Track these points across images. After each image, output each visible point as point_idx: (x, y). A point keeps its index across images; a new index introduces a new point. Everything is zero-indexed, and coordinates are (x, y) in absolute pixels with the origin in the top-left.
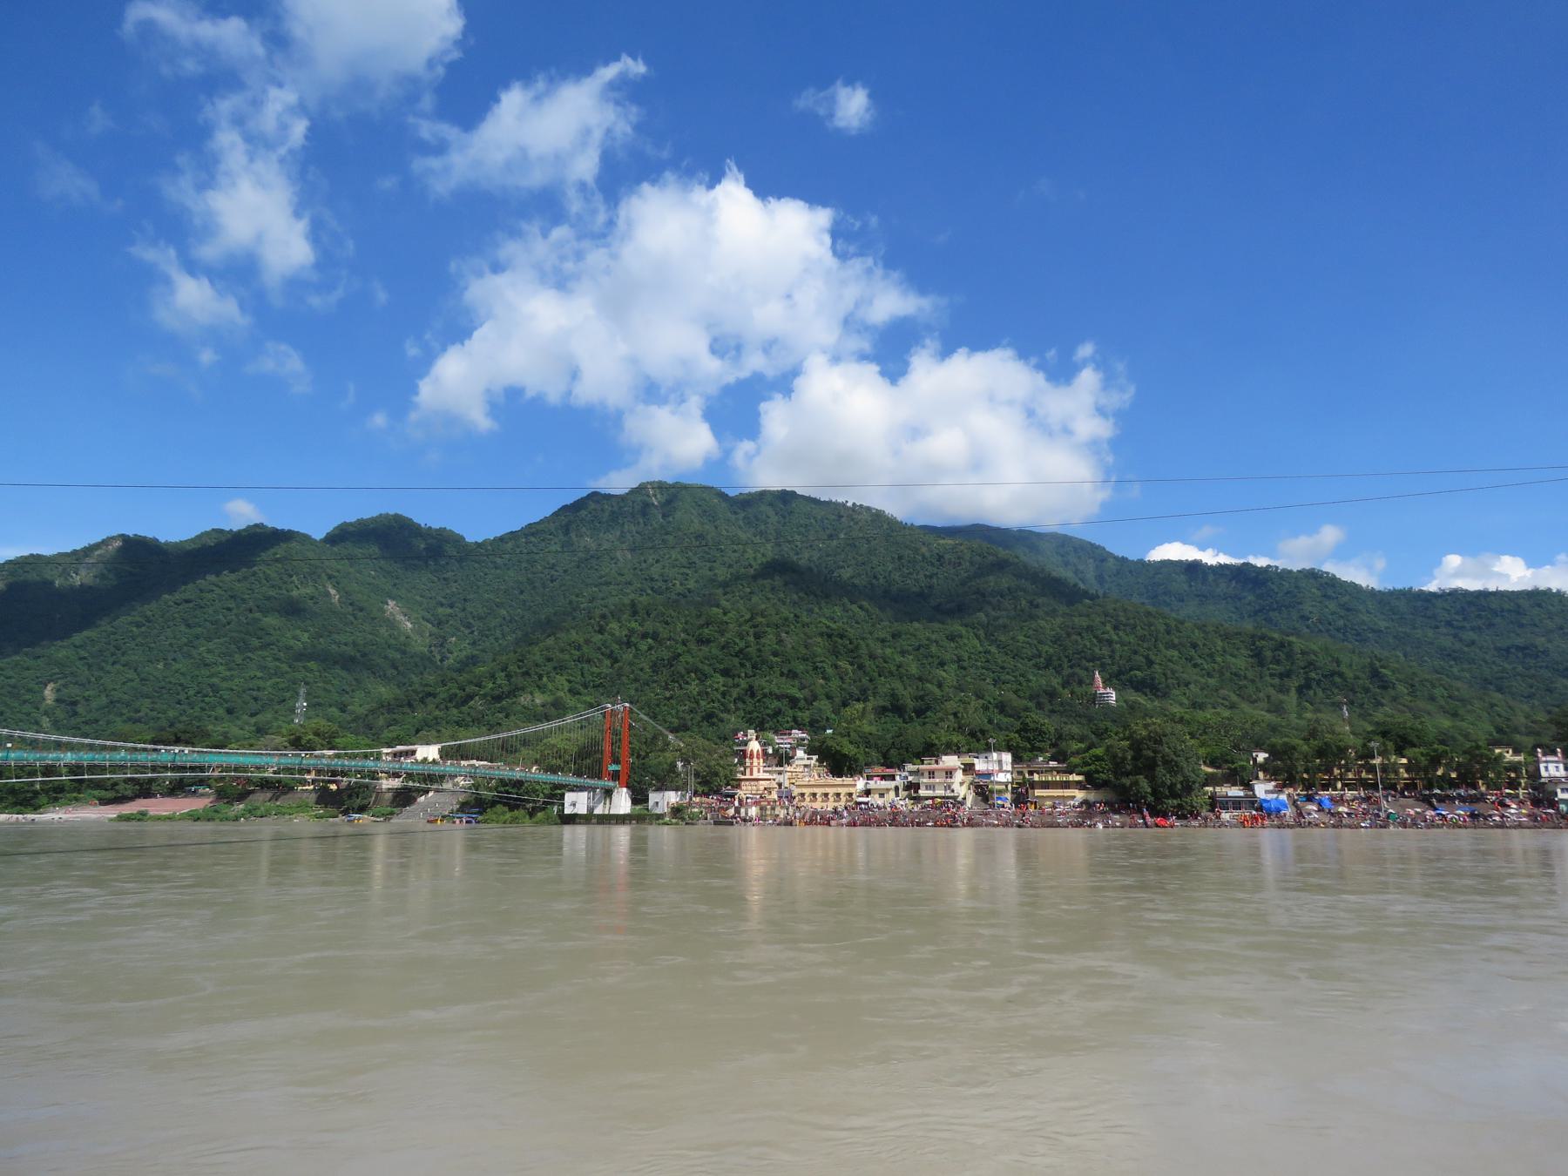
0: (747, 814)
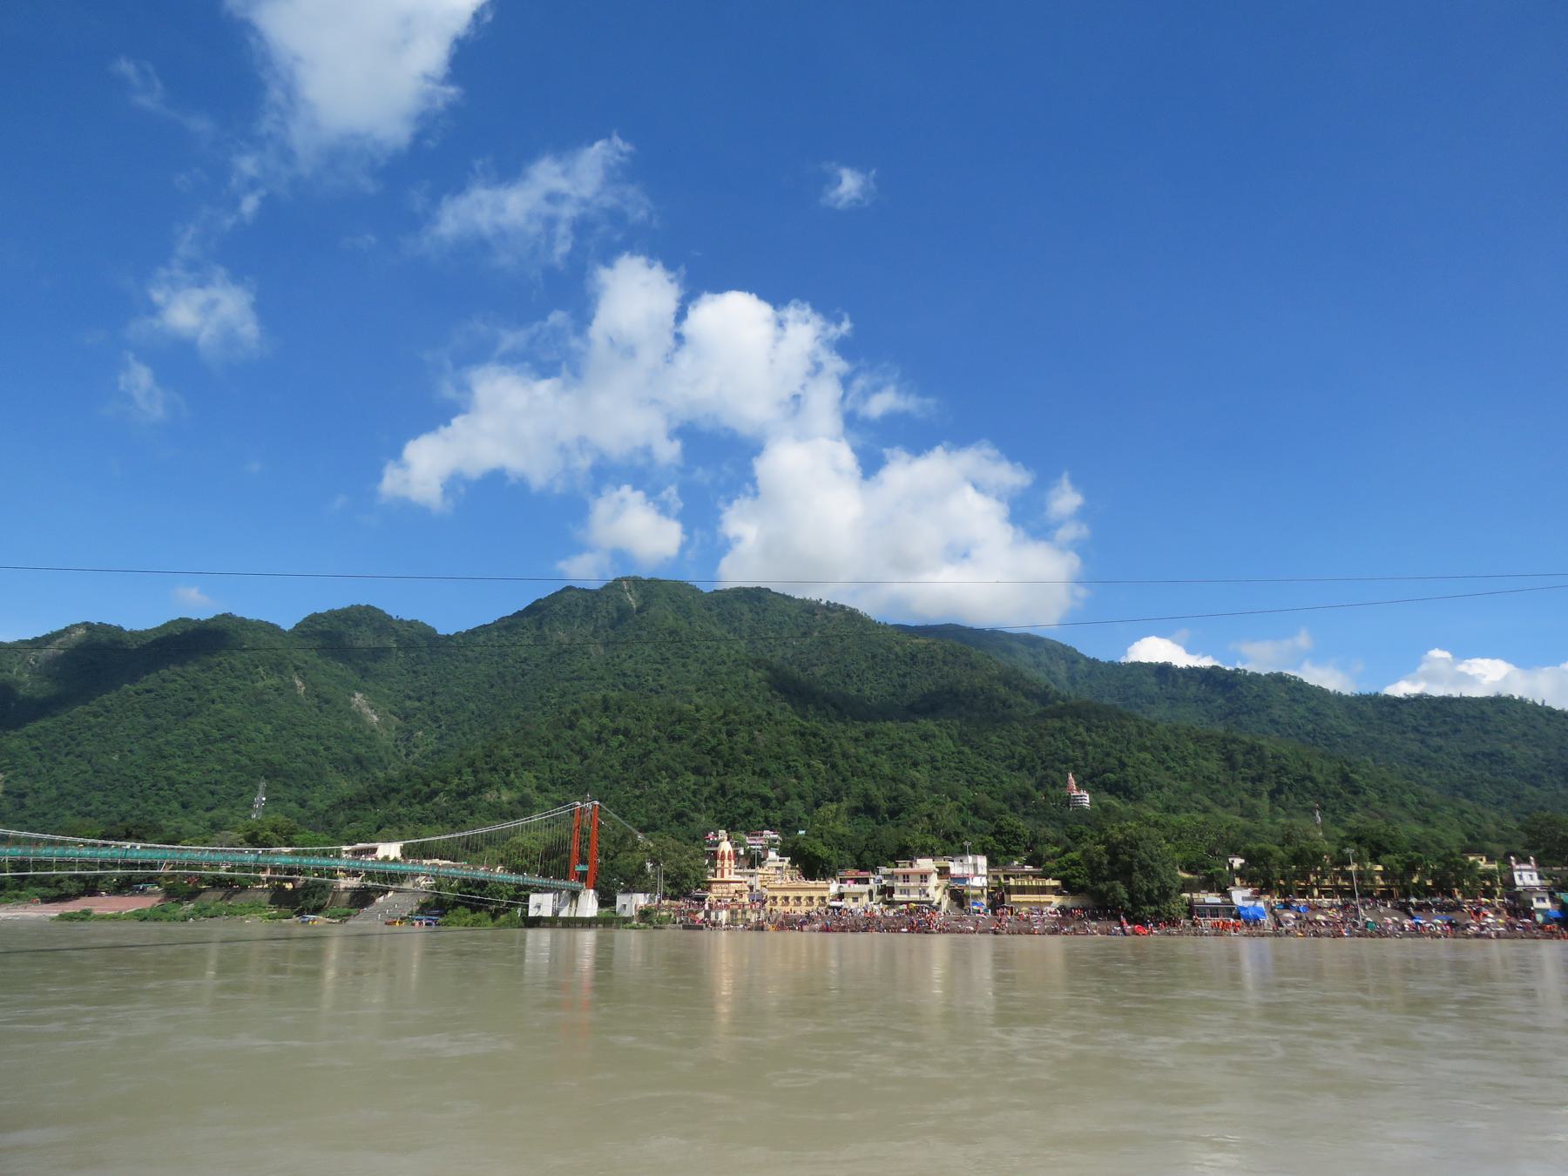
0: (717, 918)
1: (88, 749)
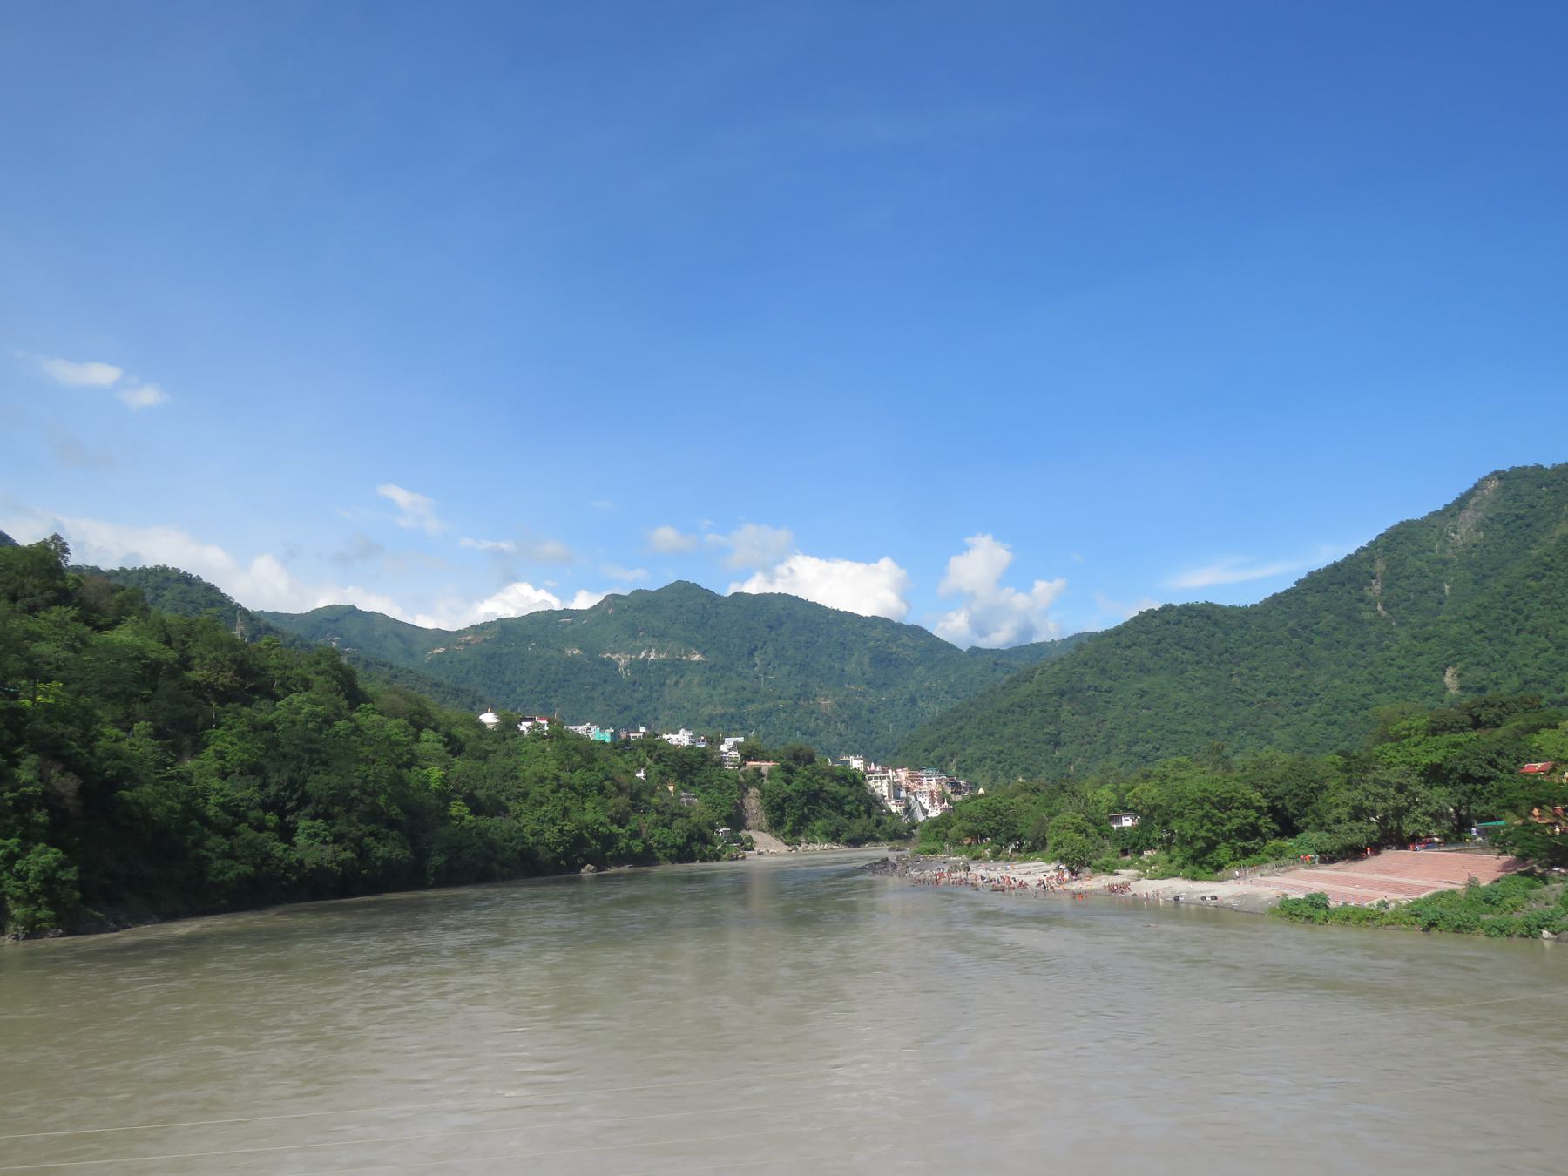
1: (1540, 621)
